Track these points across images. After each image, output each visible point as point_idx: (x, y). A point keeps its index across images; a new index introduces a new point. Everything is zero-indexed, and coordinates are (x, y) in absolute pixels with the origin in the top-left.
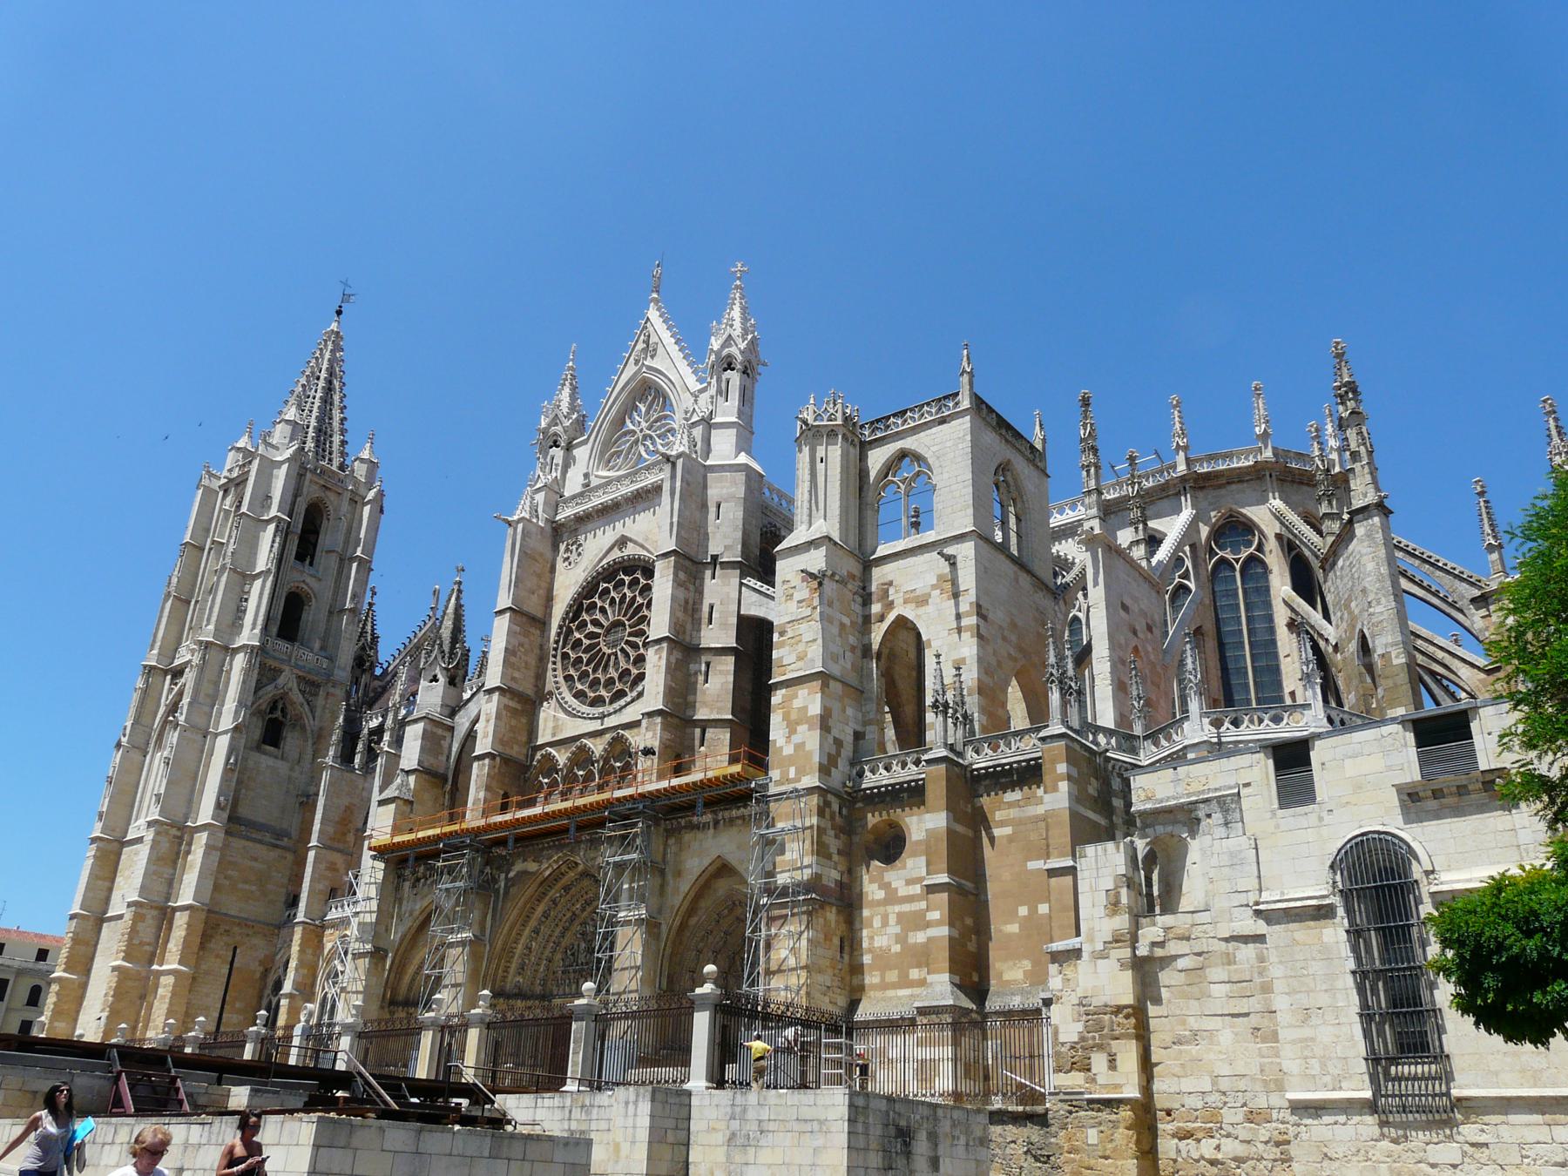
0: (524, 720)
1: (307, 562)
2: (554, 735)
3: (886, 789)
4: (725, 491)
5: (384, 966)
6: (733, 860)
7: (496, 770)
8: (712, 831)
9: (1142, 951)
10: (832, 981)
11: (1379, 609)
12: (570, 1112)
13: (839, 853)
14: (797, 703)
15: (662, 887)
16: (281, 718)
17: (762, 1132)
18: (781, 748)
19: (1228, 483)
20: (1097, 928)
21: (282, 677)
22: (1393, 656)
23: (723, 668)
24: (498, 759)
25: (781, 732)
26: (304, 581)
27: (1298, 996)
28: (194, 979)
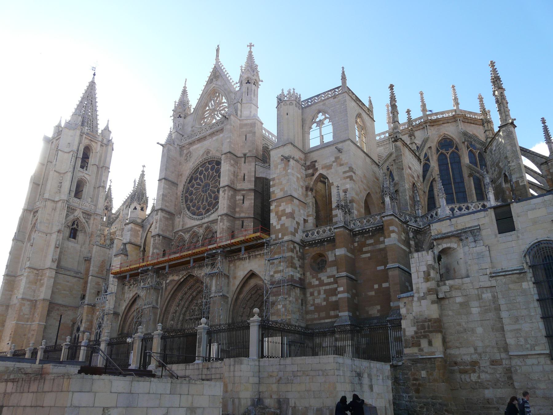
0: (171, 222)
2: (183, 227)
3: (318, 241)
4: (248, 129)
5: (118, 319)
6: (257, 271)
7: (160, 241)
8: (248, 260)
9: (441, 296)
10: (299, 317)
11: (513, 164)
12: (202, 371)
13: (300, 267)
14: (281, 208)
15: (228, 283)
16: (76, 228)
17: (294, 376)
18: (275, 226)
19: (443, 123)
20: (420, 287)
21: (76, 212)
22: (520, 182)
23: (250, 197)
24: (161, 237)
25: (275, 220)
26: (84, 176)
27: (512, 311)
28: (45, 327)
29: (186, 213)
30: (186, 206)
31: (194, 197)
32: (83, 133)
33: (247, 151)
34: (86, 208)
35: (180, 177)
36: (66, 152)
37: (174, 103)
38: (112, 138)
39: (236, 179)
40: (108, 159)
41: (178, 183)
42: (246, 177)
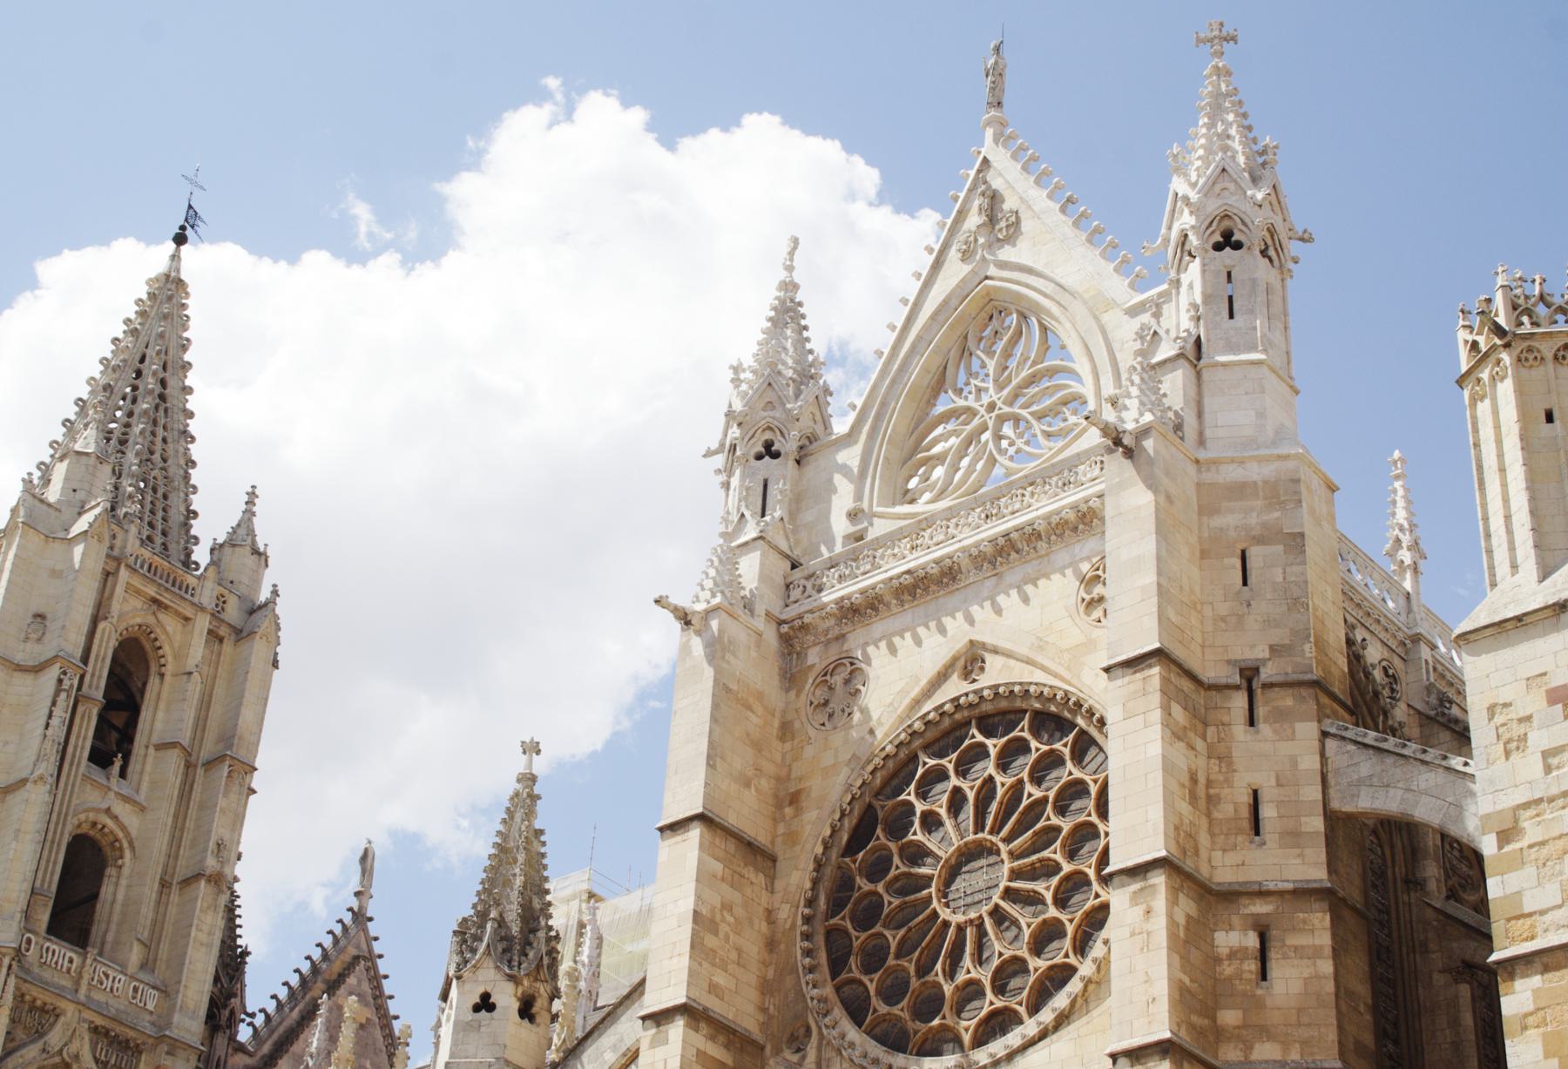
1: (118, 764)
4: (1253, 520)
21: (58, 1027)
26: (108, 811)
29: (843, 1036)
30: (838, 989)
31: (893, 938)
32: (118, 560)
33: (1261, 652)
34: (111, 1001)
35: (788, 811)
36: (20, 668)
37: (730, 374)
38: (275, 593)
39: (1204, 822)
40: (247, 715)
41: (779, 849)
42: (1267, 812)
